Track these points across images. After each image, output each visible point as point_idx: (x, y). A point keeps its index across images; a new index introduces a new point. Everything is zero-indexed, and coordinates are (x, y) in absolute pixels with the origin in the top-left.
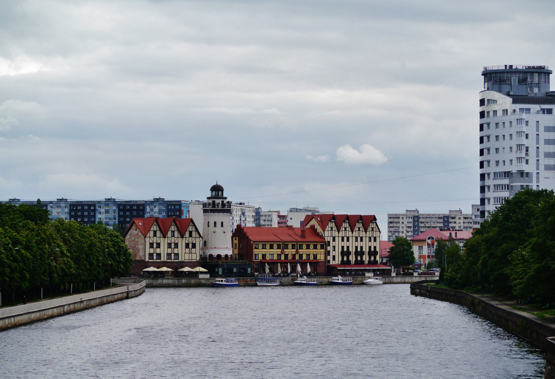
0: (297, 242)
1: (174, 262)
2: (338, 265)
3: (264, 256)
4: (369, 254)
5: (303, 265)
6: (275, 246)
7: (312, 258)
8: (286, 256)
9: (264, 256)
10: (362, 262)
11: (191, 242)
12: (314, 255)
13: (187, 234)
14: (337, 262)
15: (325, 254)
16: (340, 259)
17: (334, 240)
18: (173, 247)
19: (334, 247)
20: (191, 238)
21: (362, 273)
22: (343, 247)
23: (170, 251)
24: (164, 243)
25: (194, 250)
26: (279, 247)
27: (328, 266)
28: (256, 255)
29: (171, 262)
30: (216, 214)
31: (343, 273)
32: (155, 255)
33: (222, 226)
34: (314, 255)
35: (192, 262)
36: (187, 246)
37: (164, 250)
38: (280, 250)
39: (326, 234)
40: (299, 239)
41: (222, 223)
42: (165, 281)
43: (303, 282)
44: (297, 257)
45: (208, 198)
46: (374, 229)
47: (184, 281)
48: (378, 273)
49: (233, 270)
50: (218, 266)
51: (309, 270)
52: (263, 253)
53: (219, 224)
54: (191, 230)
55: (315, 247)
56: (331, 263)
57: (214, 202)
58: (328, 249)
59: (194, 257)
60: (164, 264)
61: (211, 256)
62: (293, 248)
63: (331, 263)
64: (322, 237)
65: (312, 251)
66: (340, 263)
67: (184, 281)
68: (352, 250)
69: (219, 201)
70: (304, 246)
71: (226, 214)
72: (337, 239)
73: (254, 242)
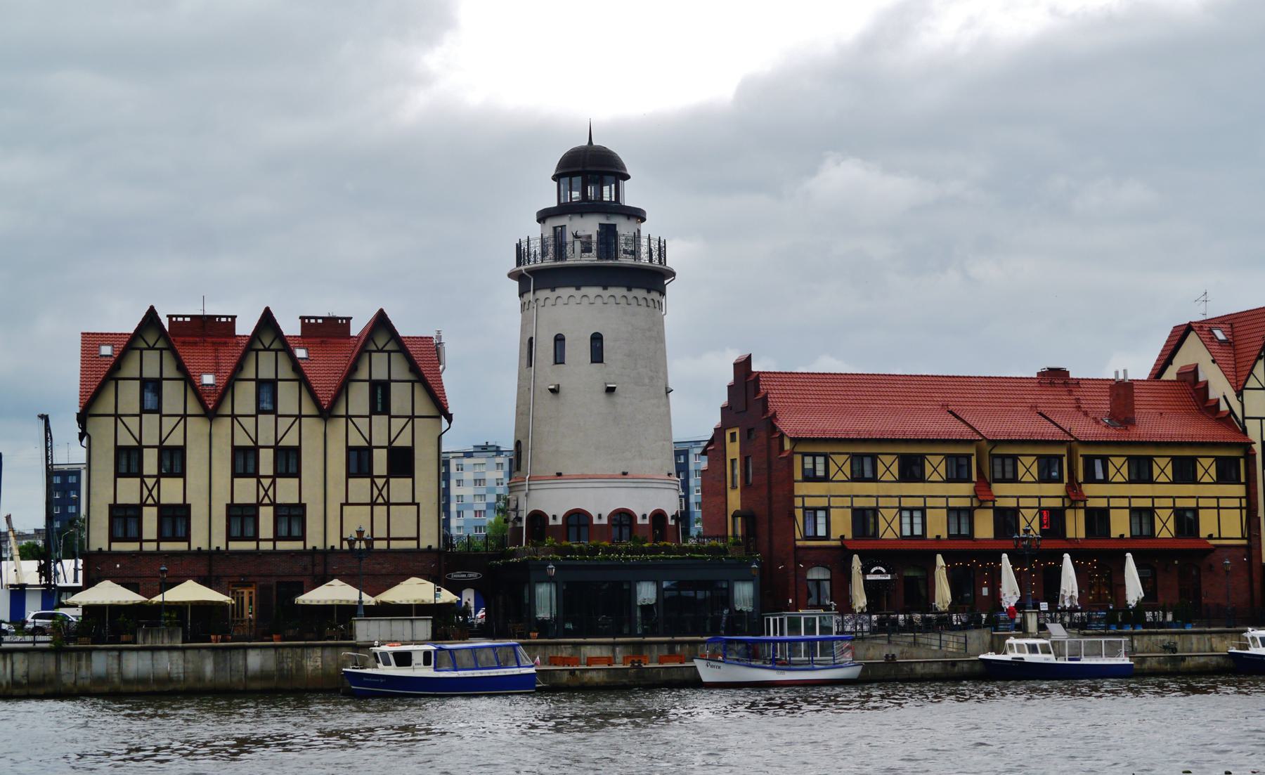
0: (1072, 443)
1: (275, 553)
5: (1101, 566)
6: (935, 466)
7: (1165, 527)
8: (1006, 519)
9: (864, 518)
11: (380, 438)
12: (1179, 513)
13: (359, 398)
24: (208, 451)
25: (400, 488)
26: (957, 474)
30: (565, 292)
32: (266, 515)
34: (1179, 513)
35: (388, 551)
36: (359, 462)
37: (208, 490)
38: (966, 489)
40: (1084, 428)
41: (597, 339)
42: (136, 664)
43: (1029, 657)
44: (1076, 526)
45: (543, 216)
47: (255, 660)
49: (632, 593)
50: (527, 574)
51: (1134, 590)
52: (859, 503)
53: (578, 349)
54: (380, 374)
55: (1185, 472)
57: (559, 234)
59: (403, 522)
60: (207, 567)
61: (538, 518)
62: (1044, 478)
65: (1164, 493)
67: (255, 660)
69: (589, 226)
70: (1119, 467)
71: (619, 292)
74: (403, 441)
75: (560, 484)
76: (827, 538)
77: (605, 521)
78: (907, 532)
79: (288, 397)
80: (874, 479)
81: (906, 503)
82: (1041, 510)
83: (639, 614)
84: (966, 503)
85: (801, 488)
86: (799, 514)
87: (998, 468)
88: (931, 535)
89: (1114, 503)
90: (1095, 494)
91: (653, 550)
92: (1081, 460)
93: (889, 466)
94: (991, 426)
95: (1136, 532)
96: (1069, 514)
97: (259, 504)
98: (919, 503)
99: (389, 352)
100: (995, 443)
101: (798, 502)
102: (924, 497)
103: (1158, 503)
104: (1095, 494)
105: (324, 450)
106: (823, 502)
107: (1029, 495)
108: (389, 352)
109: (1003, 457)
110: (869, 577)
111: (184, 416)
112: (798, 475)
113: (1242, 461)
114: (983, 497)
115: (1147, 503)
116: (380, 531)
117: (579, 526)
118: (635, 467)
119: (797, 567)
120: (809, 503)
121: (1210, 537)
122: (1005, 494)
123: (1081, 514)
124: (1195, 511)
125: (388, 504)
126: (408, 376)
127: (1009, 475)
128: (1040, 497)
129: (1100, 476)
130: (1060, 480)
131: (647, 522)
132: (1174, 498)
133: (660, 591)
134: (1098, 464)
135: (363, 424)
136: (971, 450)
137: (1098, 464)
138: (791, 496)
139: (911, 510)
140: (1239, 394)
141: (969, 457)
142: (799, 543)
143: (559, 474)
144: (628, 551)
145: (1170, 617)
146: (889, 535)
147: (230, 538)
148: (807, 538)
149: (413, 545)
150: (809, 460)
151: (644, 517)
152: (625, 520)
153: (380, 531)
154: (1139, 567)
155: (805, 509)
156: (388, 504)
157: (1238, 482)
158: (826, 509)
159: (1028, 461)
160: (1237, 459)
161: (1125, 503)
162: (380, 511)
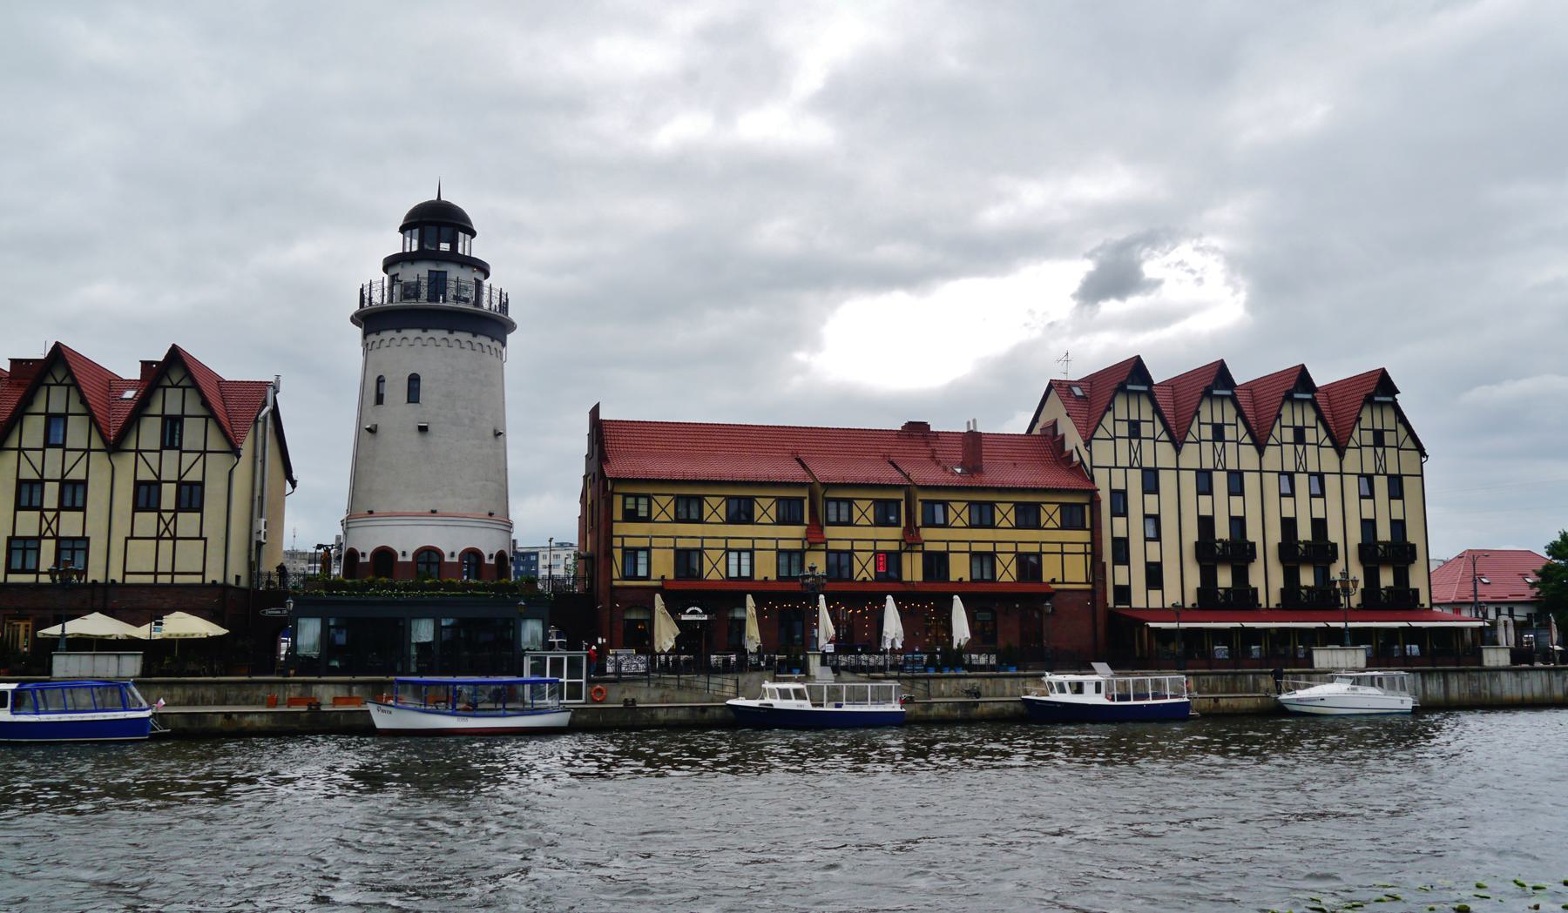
0: (909, 489)
2: (1178, 612)
6: (765, 508)
7: (1007, 572)
8: (841, 561)
9: (686, 559)
10: (1325, 598)
11: (169, 473)
12: (1022, 558)
13: (150, 432)
14: (1171, 595)
16: (1194, 579)
17: (1151, 482)
18: (51, 500)
19: (1157, 519)
20: (170, 456)
21: (1290, 655)
22: (1206, 524)
25: (187, 523)
27: (1112, 614)
28: (631, 554)
29: (37, 586)
31: (1187, 650)
34: (1022, 558)
35: (172, 585)
36: (146, 496)
38: (797, 531)
39: (1102, 452)
41: (414, 380)
44: (913, 570)
46: (1389, 439)
48: (1415, 649)
51: (961, 630)
52: (682, 544)
54: (173, 409)
55: (1028, 517)
56: (1138, 600)
58: (1120, 532)
59: (189, 558)
62: (881, 522)
63: (1138, 600)
64: (1084, 472)
65: (1007, 538)
66: (1191, 599)
68: (1265, 535)
70: (959, 511)
72: (1166, 480)
73: (618, 481)
74: (194, 475)
76: (647, 578)
77: (409, 559)
78: (733, 573)
79: (77, 432)
80: (700, 521)
81: (732, 544)
82: (876, 553)
83: (414, 652)
84: (797, 545)
85: (620, 528)
86: (618, 554)
88: (757, 577)
89: (953, 547)
90: (934, 539)
91: (436, 587)
92: (919, 505)
93: (715, 507)
94: (825, 471)
95: (976, 575)
96: (906, 558)
97: (41, 537)
98: (748, 544)
99: (184, 388)
100: (828, 486)
101: (617, 542)
102: (753, 539)
103: (999, 547)
104: (934, 539)
106: (644, 543)
107: (863, 539)
108: (184, 388)
109: (838, 501)
110: (684, 618)
112: (618, 514)
113: (1087, 508)
114: (814, 539)
115: (989, 548)
116: (165, 566)
117: (428, 564)
118: (446, 505)
119: (612, 607)
120: (629, 543)
121: (1053, 581)
122: (838, 537)
123: (918, 558)
124: (1039, 555)
125: (174, 538)
126: (201, 411)
127: (844, 518)
128: (875, 541)
129: (940, 519)
130: (898, 524)
131: (456, 560)
132: (1016, 543)
133: (438, 629)
134: (939, 509)
135: (153, 458)
136: (805, 493)
137: (939, 509)
138: (610, 536)
139: (739, 551)
140: (1088, 443)
141: (801, 500)
142: (616, 583)
143: (371, 512)
144: (407, 588)
145: (993, 661)
146: (714, 576)
148: (625, 578)
149: (198, 579)
150: (630, 501)
151: (452, 555)
152: (473, 559)
153: (165, 566)
154: (900, 609)
155: (625, 550)
156: (174, 538)
157: (1084, 528)
158: (648, 550)
159: (864, 505)
160: (1082, 506)
161: (965, 547)
162: (166, 545)
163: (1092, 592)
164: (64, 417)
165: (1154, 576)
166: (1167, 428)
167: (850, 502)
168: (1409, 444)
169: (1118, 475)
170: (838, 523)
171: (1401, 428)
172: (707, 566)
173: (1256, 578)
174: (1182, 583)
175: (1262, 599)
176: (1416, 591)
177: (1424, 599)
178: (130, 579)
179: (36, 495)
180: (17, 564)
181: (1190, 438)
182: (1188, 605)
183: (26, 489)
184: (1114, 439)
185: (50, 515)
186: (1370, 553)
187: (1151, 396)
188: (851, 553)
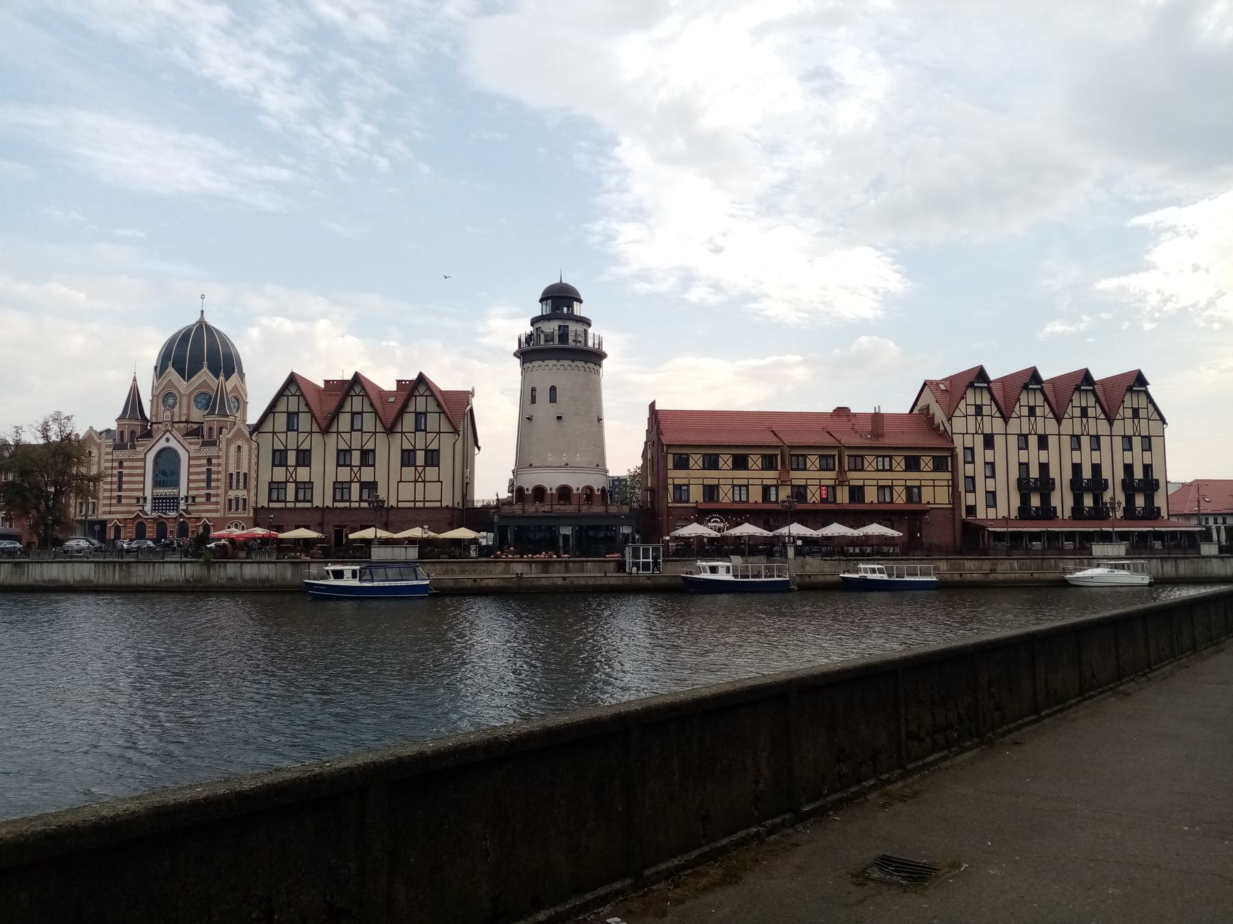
0: (840, 448)
2: (1006, 520)
3: (711, 491)
4: (1072, 489)
6: (755, 461)
7: (900, 498)
9: (711, 491)
10: (1100, 512)
12: (909, 489)
14: (1002, 512)
15: (954, 486)
16: (1016, 502)
17: (989, 442)
19: (993, 465)
22: (1024, 466)
23: (344, 474)
24: (324, 452)
25: (431, 472)
26: (769, 463)
27: (965, 524)
28: (678, 487)
29: (350, 509)
33: (553, 399)
35: (424, 508)
36: (408, 458)
37: (323, 474)
39: (958, 425)
41: (553, 389)
46: (1142, 413)
52: (707, 482)
54: (421, 409)
58: (970, 473)
59: (433, 492)
63: (981, 513)
64: (946, 436)
65: (900, 477)
68: (1061, 475)
72: (999, 441)
73: (669, 446)
74: (433, 446)
75: (531, 471)
85: (671, 473)
86: (671, 488)
87: (795, 463)
93: (726, 461)
94: (789, 439)
97: (351, 482)
98: (745, 482)
100: (791, 447)
101: (670, 481)
104: (855, 478)
105: (388, 451)
109: (798, 456)
111: (311, 433)
116: (420, 497)
120: (677, 482)
122: (798, 477)
123: (846, 489)
125: (424, 481)
126: (437, 409)
127: (801, 466)
136: (778, 452)
139: (740, 486)
146: (726, 500)
147: (335, 500)
148: (675, 501)
149: (438, 504)
153: (420, 497)
155: (675, 486)
156: (424, 481)
159: (813, 458)
161: (875, 483)
162: (420, 485)
163: (953, 509)
164: (297, 413)
165: (991, 497)
166: (999, 409)
167: (805, 456)
168: (1155, 416)
169: (968, 438)
170: (798, 469)
171: (1150, 406)
172: (722, 495)
173: (1055, 501)
174: (1008, 504)
175: (1059, 513)
176: (1159, 508)
177: (1164, 513)
178: (401, 505)
179: (348, 458)
180: (338, 498)
181: (1014, 415)
182: (1012, 517)
183: (278, 454)
184: (966, 416)
185: (356, 469)
186: (1129, 486)
187: (989, 390)
188: (805, 487)
